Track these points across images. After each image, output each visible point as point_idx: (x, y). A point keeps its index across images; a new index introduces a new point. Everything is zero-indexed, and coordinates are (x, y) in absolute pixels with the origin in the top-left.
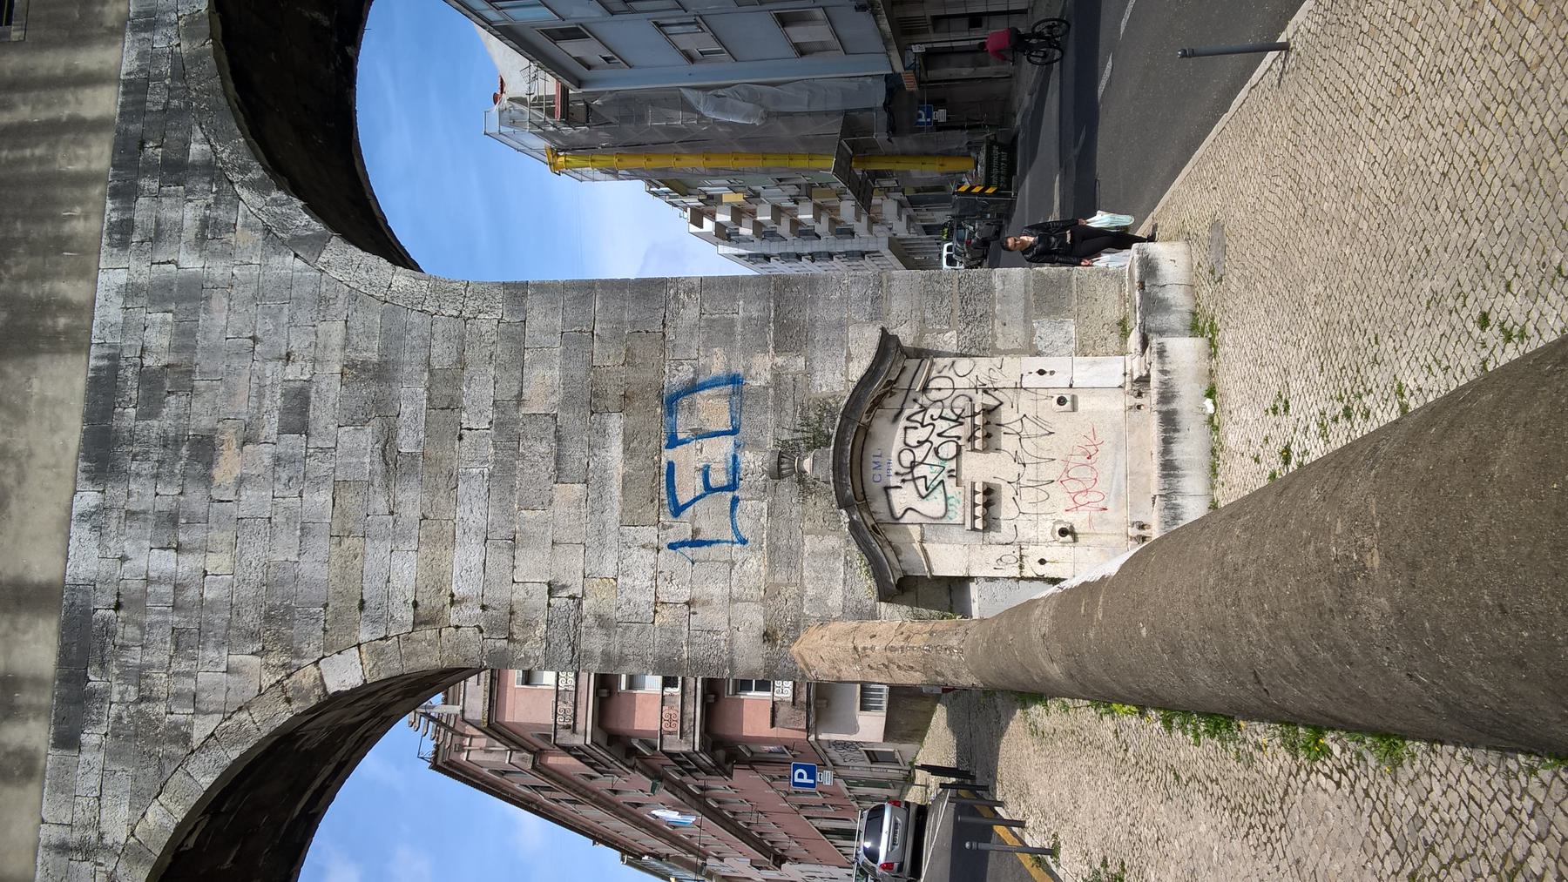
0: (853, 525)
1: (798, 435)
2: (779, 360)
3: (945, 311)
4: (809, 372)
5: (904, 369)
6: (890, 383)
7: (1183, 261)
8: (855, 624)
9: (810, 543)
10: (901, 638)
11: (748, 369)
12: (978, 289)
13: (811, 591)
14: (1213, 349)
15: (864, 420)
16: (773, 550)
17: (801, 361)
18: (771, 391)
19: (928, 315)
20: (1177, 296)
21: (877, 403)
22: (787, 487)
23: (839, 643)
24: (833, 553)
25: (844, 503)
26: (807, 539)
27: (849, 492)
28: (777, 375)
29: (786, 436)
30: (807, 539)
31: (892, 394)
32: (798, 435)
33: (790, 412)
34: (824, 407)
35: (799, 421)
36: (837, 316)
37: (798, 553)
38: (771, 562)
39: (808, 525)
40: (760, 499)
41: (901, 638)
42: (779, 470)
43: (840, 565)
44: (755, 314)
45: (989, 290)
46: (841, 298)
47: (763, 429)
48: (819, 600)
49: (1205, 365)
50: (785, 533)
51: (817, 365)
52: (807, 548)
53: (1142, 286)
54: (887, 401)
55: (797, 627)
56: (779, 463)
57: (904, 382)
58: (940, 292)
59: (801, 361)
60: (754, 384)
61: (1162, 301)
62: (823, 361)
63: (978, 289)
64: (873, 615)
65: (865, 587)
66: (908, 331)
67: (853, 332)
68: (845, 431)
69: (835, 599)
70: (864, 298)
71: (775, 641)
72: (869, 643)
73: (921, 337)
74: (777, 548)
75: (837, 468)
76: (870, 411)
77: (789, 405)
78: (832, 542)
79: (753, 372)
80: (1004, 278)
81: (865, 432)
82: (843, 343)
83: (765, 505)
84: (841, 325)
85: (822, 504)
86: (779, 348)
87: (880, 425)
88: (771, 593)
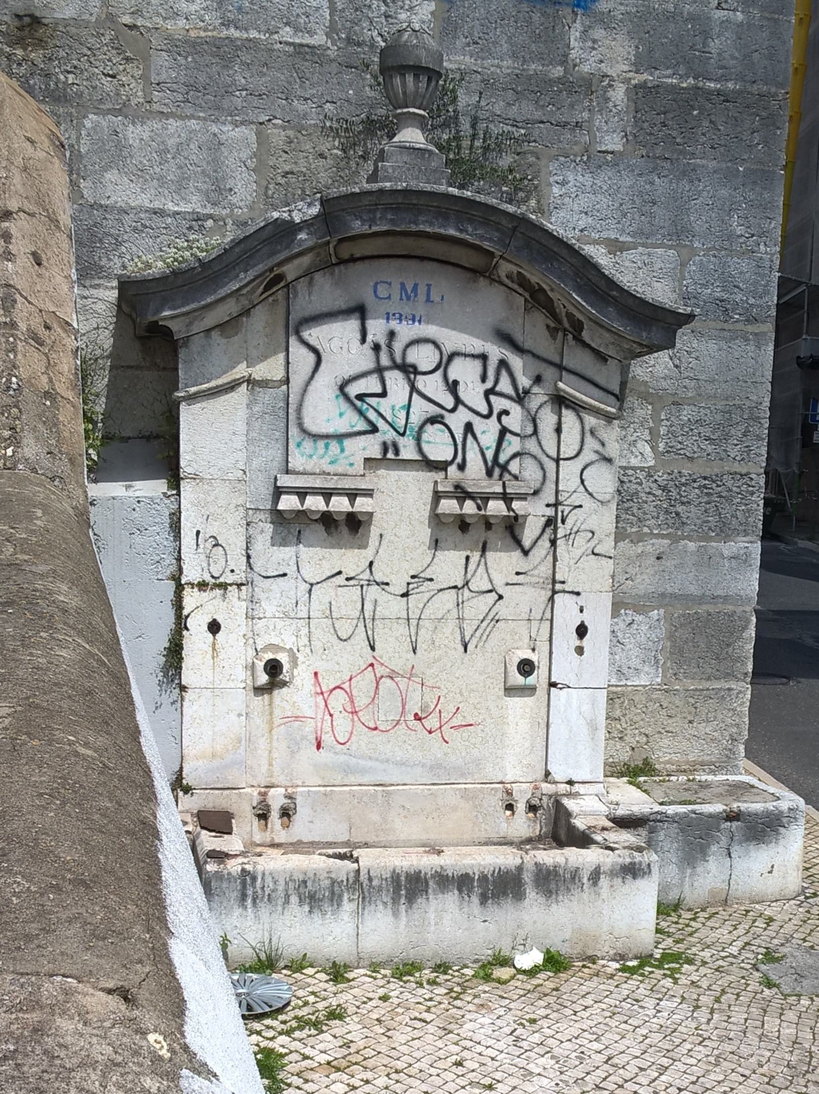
0: (283, 231)
1: (465, 126)
2: (619, 94)
3: (690, 445)
4: (594, 159)
5: (602, 358)
6: (578, 327)
7: (771, 886)
8: (65, 219)
9: (239, 137)
10: (36, 323)
11: (605, 21)
12: (727, 510)
13: (135, 133)
14: (638, 963)
15: (505, 268)
16: (223, 52)
17: (613, 142)
18: (558, 71)
19: (687, 413)
20: (710, 875)
21: (537, 299)
22: (361, 92)
23: (17, 179)
24: (219, 190)
25: (333, 211)
26: (248, 133)
27: (358, 227)
28: (591, 87)
29: (465, 100)
30: (248, 133)
31: (553, 332)
32: (465, 126)
33: (513, 112)
34: (522, 185)
35: (495, 130)
36: (699, 226)
37: (218, 110)
38: (194, 46)
39: (277, 136)
40: (332, 30)
41: (36, 323)
42: (403, 69)
43: (193, 204)
44: (714, 46)
45: (725, 532)
46: (731, 237)
47: (484, 51)
48: (116, 153)
49: (605, 948)
50: (261, 83)
51: (604, 178)
52: (229, 132)
53: (733, 816)
54: (540, 320)
55: (55, 97)
56: (418, 70)
57: (577, 359)
58: (726, 437)
59: (613, 142)
60: (574, 35)
61: (703, 852)
62: (612, 192)
63: (727, 510)
64: (88, 272)
65: (150, 257)
66: (660, 370)
67: (664, 257)
68: (486, 223)
69: (120, 190)
70: (728, 283)
71: (19, 42)
72: (21, 247)
73: (646, 397)
74: (226, 62)
75: (408, 201)
76: (523, 282)
77: (526, 109)
78: (243, 190)
79: (599, 33)
80: (741, 559)
81: (479, 270)
82: (645, 237)
83: (319, 39)
84: (679, 234)
85: (323, 169)
86: (642, 94)
87: (492, 303)
88: (130, 41)
